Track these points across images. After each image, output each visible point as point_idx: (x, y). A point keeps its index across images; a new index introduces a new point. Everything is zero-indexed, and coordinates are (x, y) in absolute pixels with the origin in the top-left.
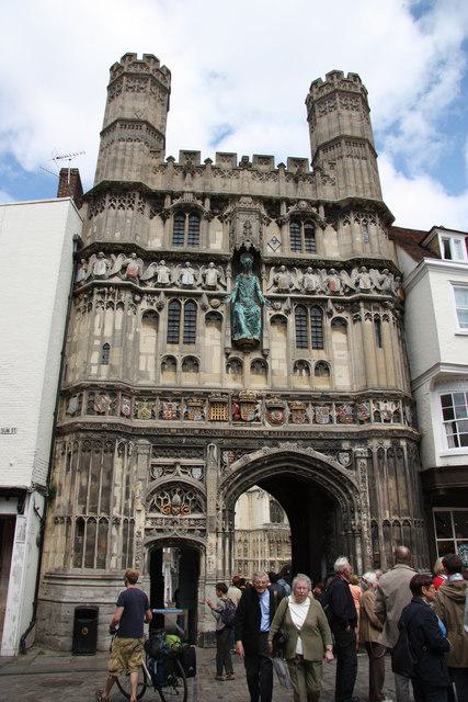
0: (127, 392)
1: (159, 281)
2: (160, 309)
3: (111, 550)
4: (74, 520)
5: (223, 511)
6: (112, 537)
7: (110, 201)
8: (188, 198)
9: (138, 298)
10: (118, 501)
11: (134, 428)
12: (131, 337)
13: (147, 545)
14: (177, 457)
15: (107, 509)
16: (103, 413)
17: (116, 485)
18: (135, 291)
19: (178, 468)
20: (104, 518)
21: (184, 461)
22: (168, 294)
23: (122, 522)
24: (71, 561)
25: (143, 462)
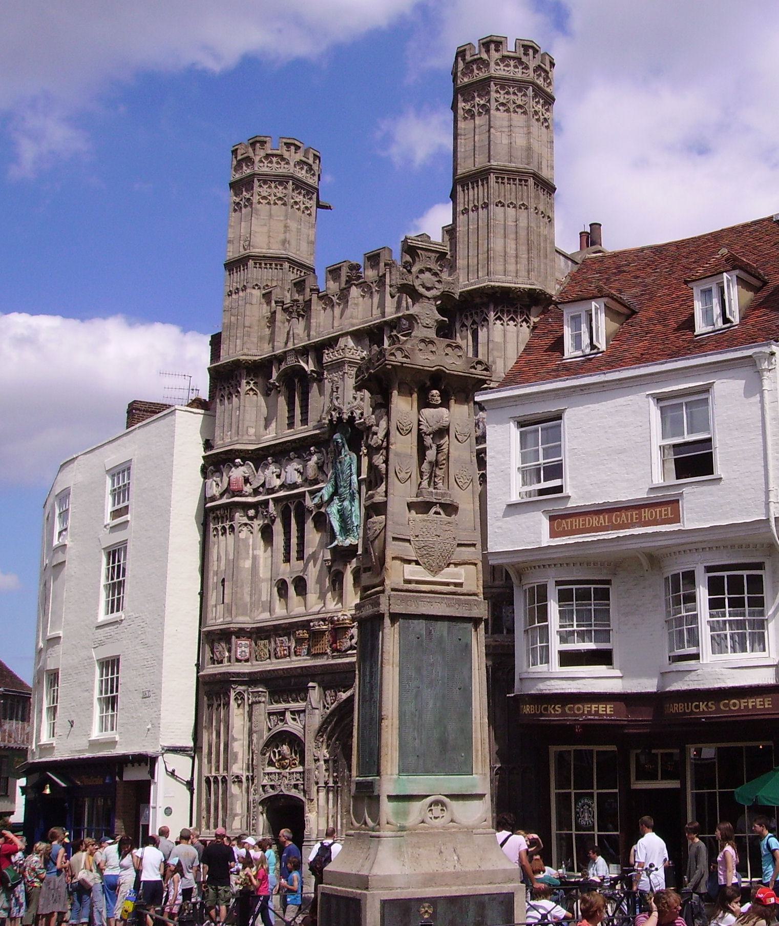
0: (241, 633)
1: (267, 486)
2: (273, 521)
3: (232, 809)
4: (204, 779)
5: (326, 761)
6: (232, 795)
7: (220, 389)
8: (291, 361)
9: (251, 512)
10: (240, 756)
11: (250, 673)
12: (248, 564)
13: (262, 803)
14: (289, 702)
15: (226, 768)
16: (221, 662)
17: (236, 740)
18: (245, 506)
19: (288, 715)
20: (224, 777)
21: (294, 705)
22: (276, 501)
23: (244, 779)
24: (204, 822)
25: (261, 711)
